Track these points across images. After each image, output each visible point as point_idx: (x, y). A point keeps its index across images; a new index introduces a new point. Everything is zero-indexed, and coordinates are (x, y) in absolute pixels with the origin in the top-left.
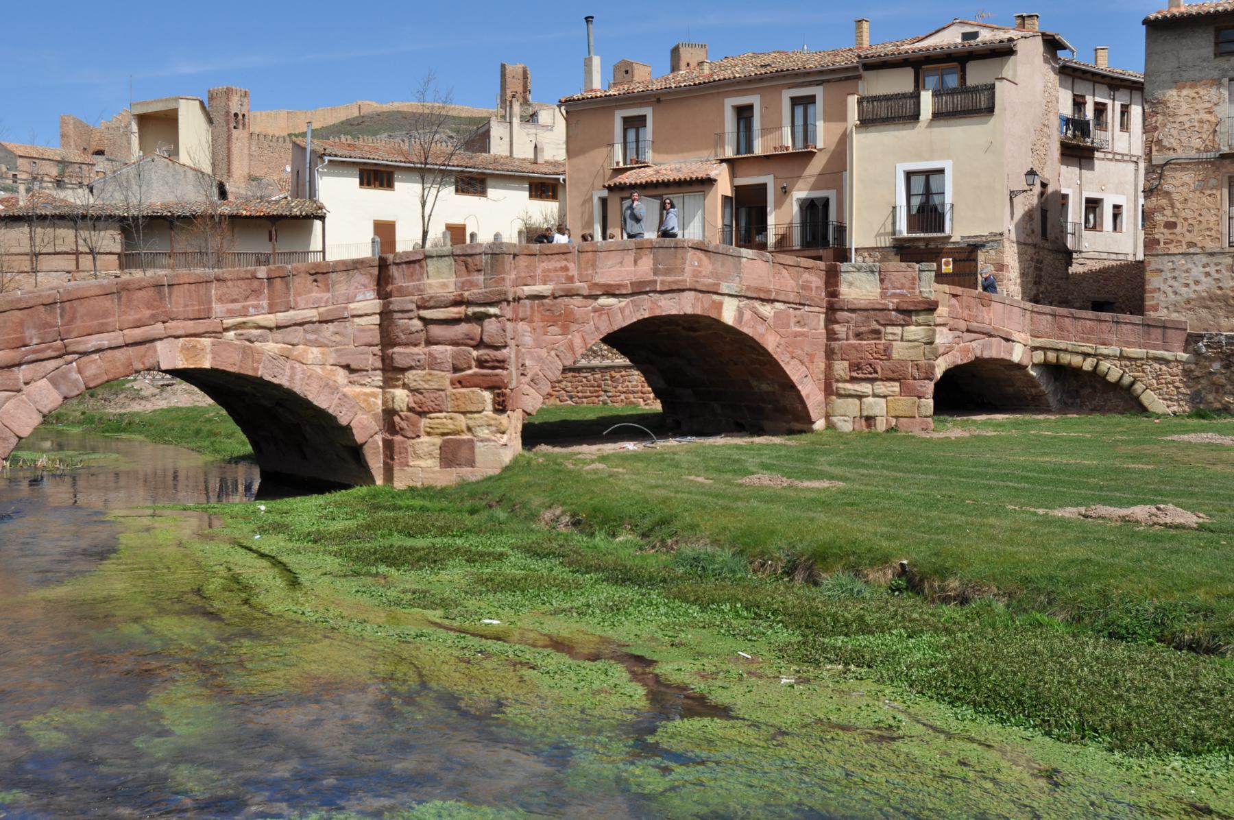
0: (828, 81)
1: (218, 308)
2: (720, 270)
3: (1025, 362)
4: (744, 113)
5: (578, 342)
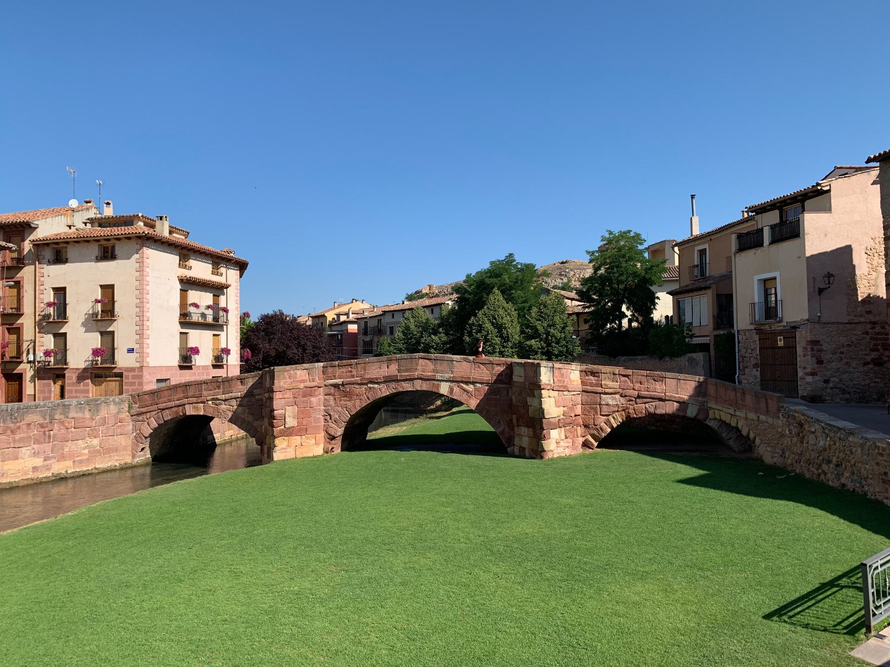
1: (205, 393)
2: (439, 368)
3: (701, 417)
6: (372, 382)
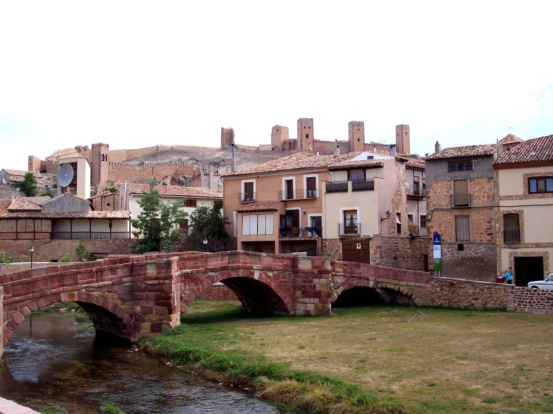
0: (320, 172)
3: (375, 287)
4: (289, 183)
5: (201, 287)
6: (212, 270)
